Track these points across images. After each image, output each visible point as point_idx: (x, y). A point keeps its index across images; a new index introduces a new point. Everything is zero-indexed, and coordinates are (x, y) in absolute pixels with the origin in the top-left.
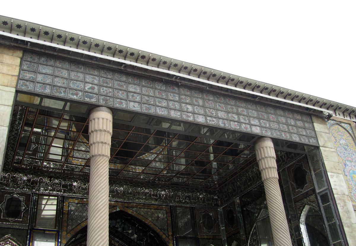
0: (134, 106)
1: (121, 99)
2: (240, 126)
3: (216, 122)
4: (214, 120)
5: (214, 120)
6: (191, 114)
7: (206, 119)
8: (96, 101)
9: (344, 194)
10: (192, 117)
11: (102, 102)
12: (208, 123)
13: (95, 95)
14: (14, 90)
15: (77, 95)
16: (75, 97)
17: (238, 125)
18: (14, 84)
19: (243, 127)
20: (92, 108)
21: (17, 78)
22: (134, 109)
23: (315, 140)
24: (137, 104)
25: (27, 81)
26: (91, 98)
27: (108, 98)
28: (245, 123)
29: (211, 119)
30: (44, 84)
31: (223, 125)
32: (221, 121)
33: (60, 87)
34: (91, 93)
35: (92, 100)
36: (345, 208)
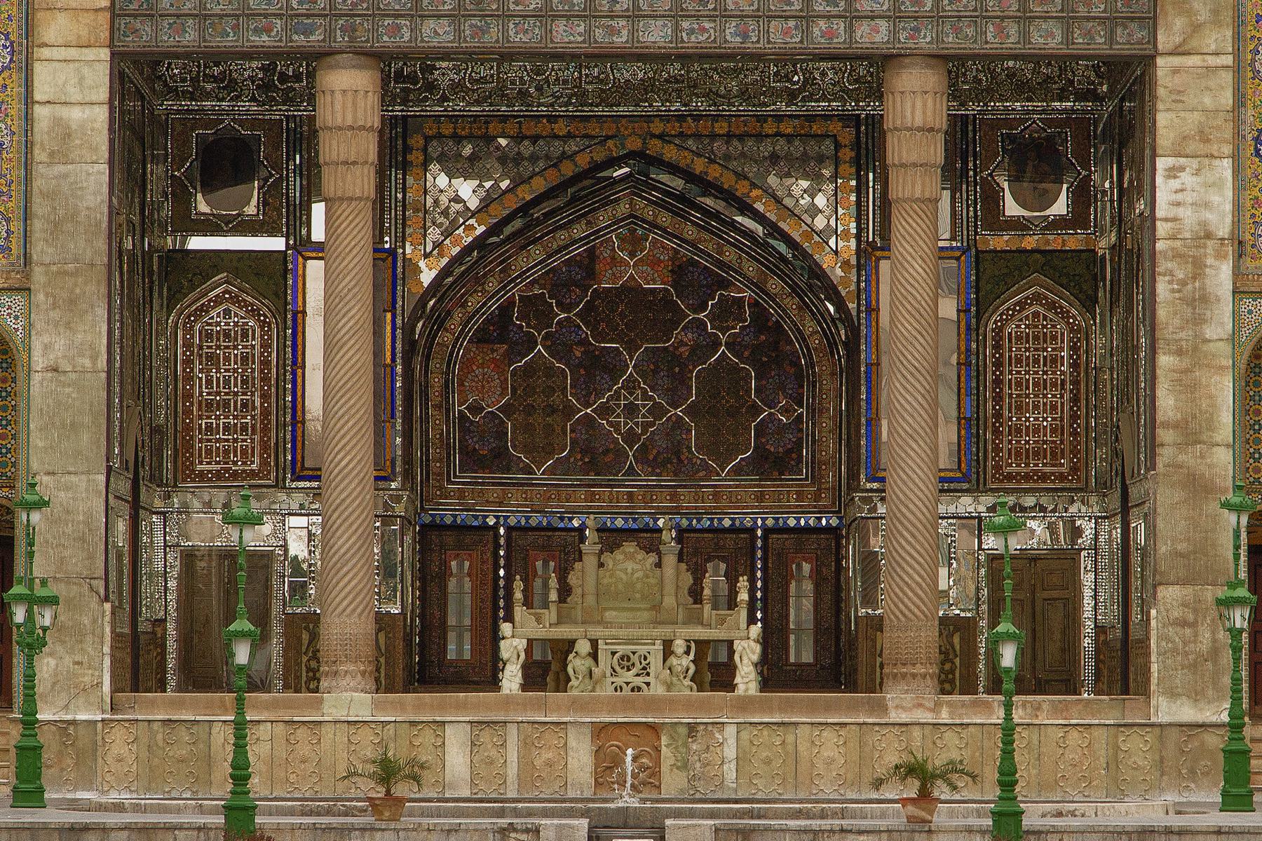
0: (436, 31)
1: (397, 16)
2: (807, 32)
3: (712, 31)
4: (707, 25)
5: (707, 25)
6: (622, 22)
7: (677, 29)
8: (324, 40)
9: (1208, 236)
10: (625, 32)
11: (341, 39)
12: (683, 41)
13: (318, 21)
14: (105, 54)
15: (268, 30)
16: (265, 38)
17: (796, 27)
18: (104, 35)
19: (816, 31)
20: (317, 58)
21: (108, 15)
22: (435, 42)
23: (1141, 28)
24: (444, 21)
25: (135, 16)
26: (307, 32)
27: (358, 20)
28: (828, 17)
29: (696, 26)
30: (178, 16)
31: (739, 39)
32: (734, 24)
33: (221, 16)
34: (308, 16)
35: (312, 38)
36: (1190, 287)
